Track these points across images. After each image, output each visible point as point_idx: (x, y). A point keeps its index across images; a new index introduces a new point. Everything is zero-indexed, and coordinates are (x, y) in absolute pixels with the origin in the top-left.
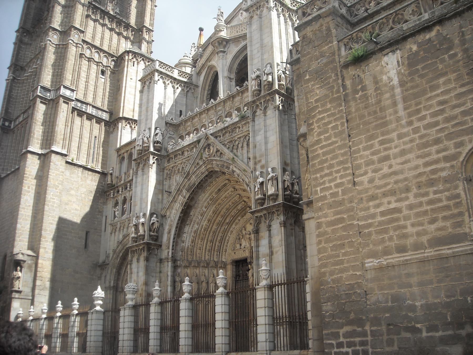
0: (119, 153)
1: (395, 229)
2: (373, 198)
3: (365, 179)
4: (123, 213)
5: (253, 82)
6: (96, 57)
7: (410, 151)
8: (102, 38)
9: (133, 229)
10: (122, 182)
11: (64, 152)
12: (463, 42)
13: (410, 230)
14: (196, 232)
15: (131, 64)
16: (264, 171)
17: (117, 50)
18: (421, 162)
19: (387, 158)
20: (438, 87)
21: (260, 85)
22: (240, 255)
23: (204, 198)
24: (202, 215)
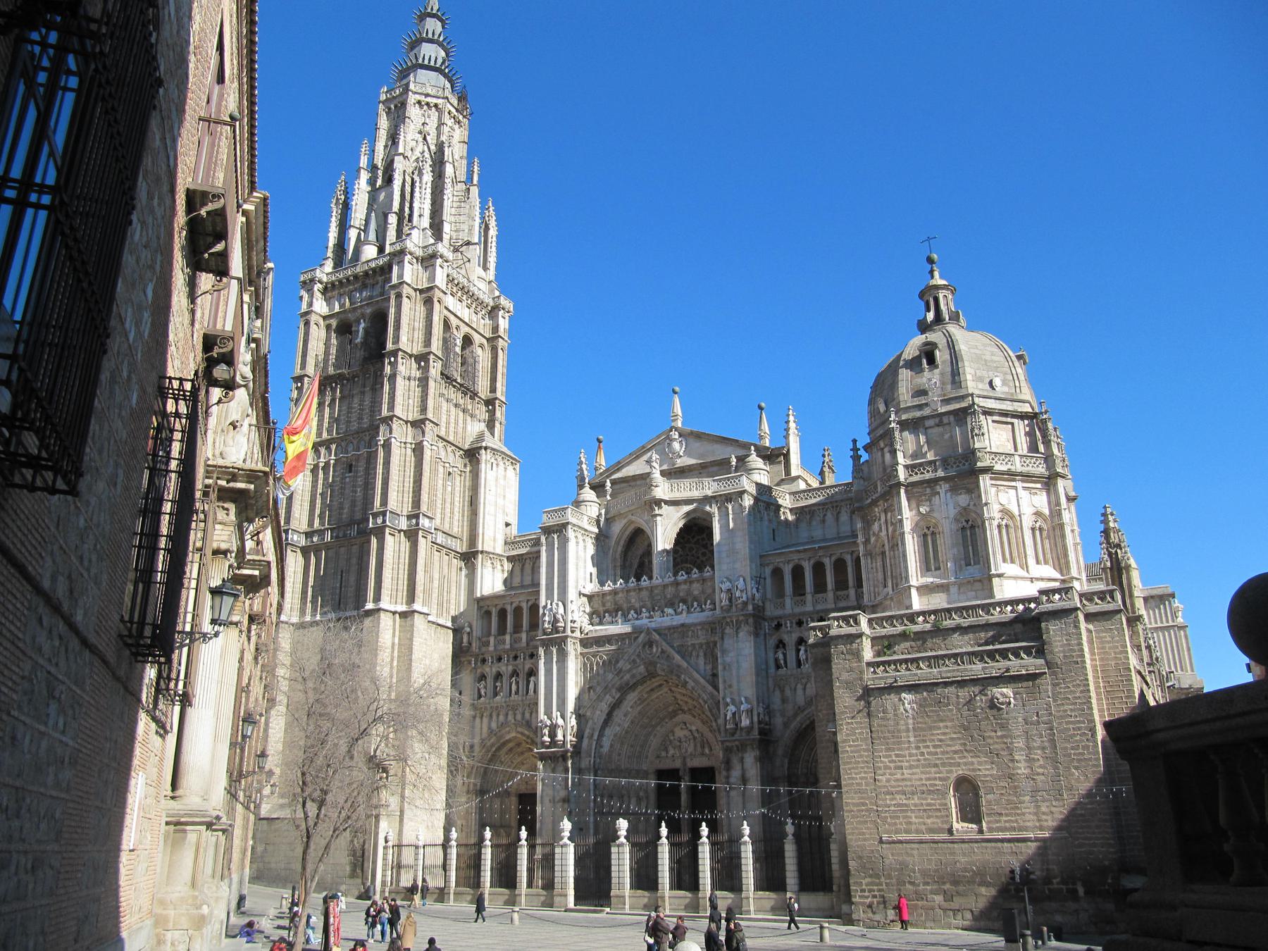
0: (482, 604)
1: (905, 817)
2: (888, 793)
3: (884, 778)
4: (496, 694)
5: (723, 595)
6: (443, 454)
7: (917, 767)
8: (448, 423)
9: (546, 731)
10: (491, 648)
11: (425, 610)
12: (958, 703)
13: (914, 820)
14: (615, 735)
15: (489, 466)
16: (736, 698)
17: (464, 438)
18: (923, 776)
19: (901, 768)
20: (939, 728)
21: (730, 600)
22: (667, 765)
23: (632, 697)
24: (625, 715)
